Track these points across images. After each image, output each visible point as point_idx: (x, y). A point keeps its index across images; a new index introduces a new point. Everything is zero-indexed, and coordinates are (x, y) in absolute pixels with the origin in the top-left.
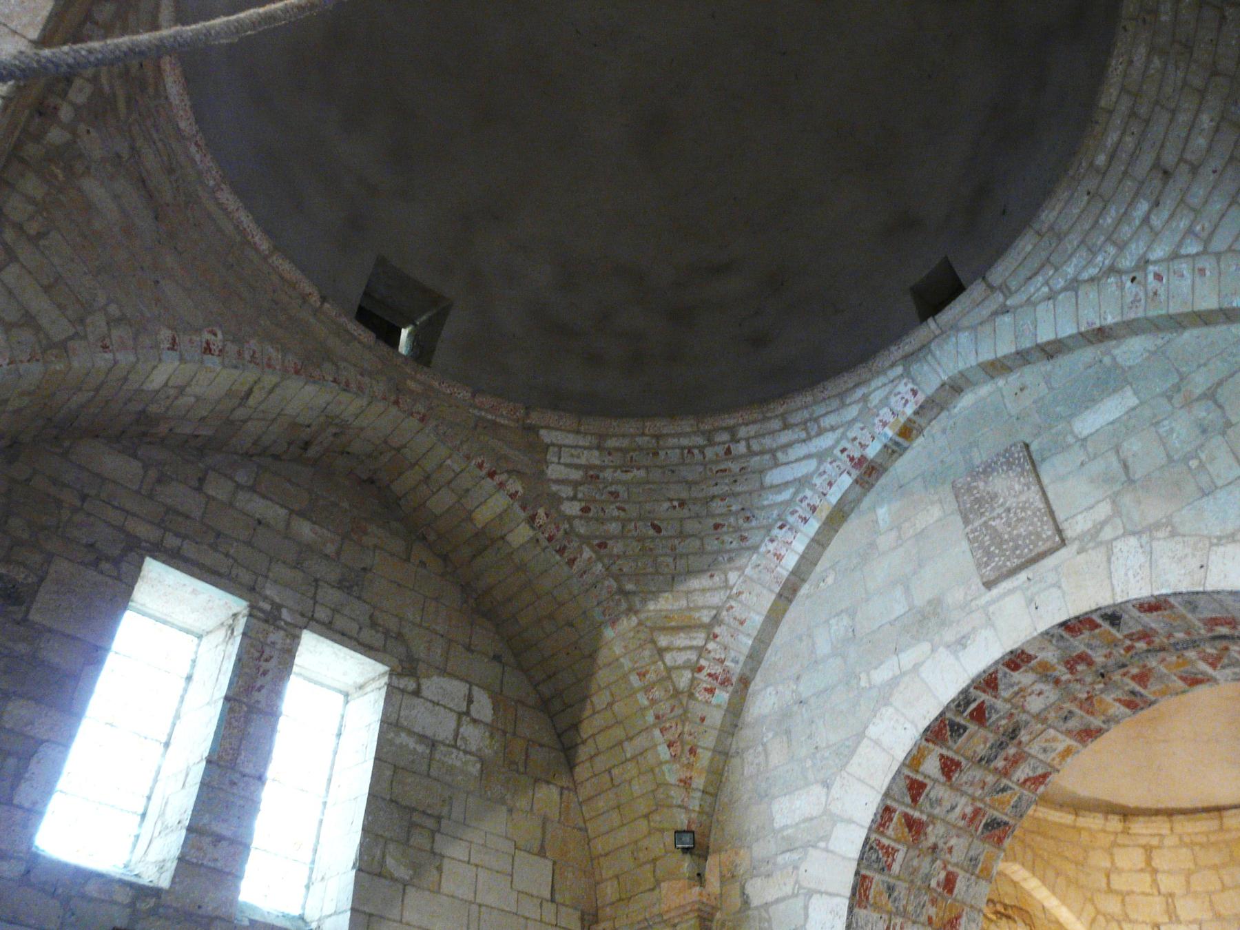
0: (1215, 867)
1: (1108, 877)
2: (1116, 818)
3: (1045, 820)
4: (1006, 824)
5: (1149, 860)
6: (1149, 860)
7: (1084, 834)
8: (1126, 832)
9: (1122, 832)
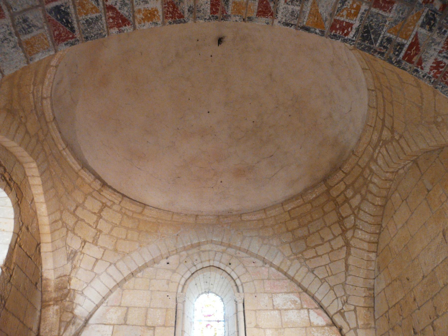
0: (128, 229)
1: (77, 207)
2: (99, 182)
3: (65, 159)
4: (72, 30)
5: (101, 210)
6: (101, 210)
7: (79, 180)
8: (99, 192)
9: (97, 191)
